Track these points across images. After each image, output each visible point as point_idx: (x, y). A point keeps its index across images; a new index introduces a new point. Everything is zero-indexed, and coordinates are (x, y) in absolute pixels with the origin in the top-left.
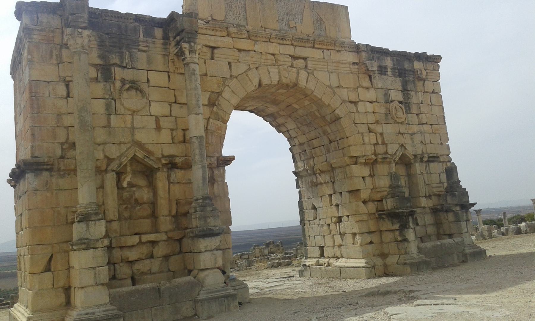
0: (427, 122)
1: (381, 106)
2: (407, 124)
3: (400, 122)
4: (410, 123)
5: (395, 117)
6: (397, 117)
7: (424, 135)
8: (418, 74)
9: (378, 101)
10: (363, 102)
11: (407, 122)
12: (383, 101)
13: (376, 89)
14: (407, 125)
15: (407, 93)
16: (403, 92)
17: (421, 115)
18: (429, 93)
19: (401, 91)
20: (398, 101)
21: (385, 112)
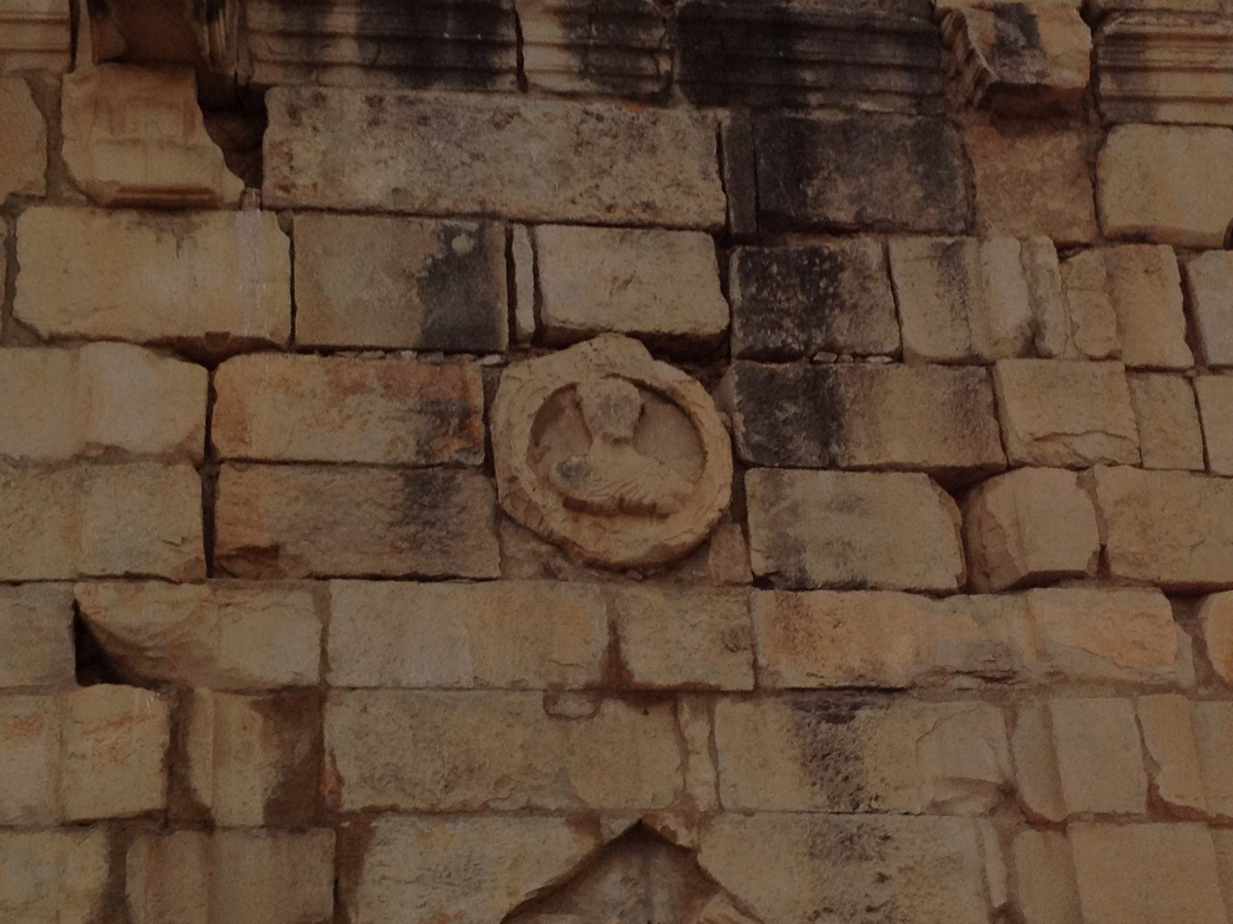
0: (1102, 556)
1: (358, 388)
2: (762, 582)
3: (622, 553)
4: (820, 569)
5: (550, 502)
6: (576, 507)
7: (1046, 714)
8: (971, 55)
9: (303, 338)
10: (57, 356)
11: (760, 565)
12: (409, 334)
13: (297, 219)
14: (764, 600)
15: (815, 253)
16: (743, 240)
17: (1007, 480)
18: (1166, 253)
19: (723, 239)
20: (633, 335)
21: (407, 454)
